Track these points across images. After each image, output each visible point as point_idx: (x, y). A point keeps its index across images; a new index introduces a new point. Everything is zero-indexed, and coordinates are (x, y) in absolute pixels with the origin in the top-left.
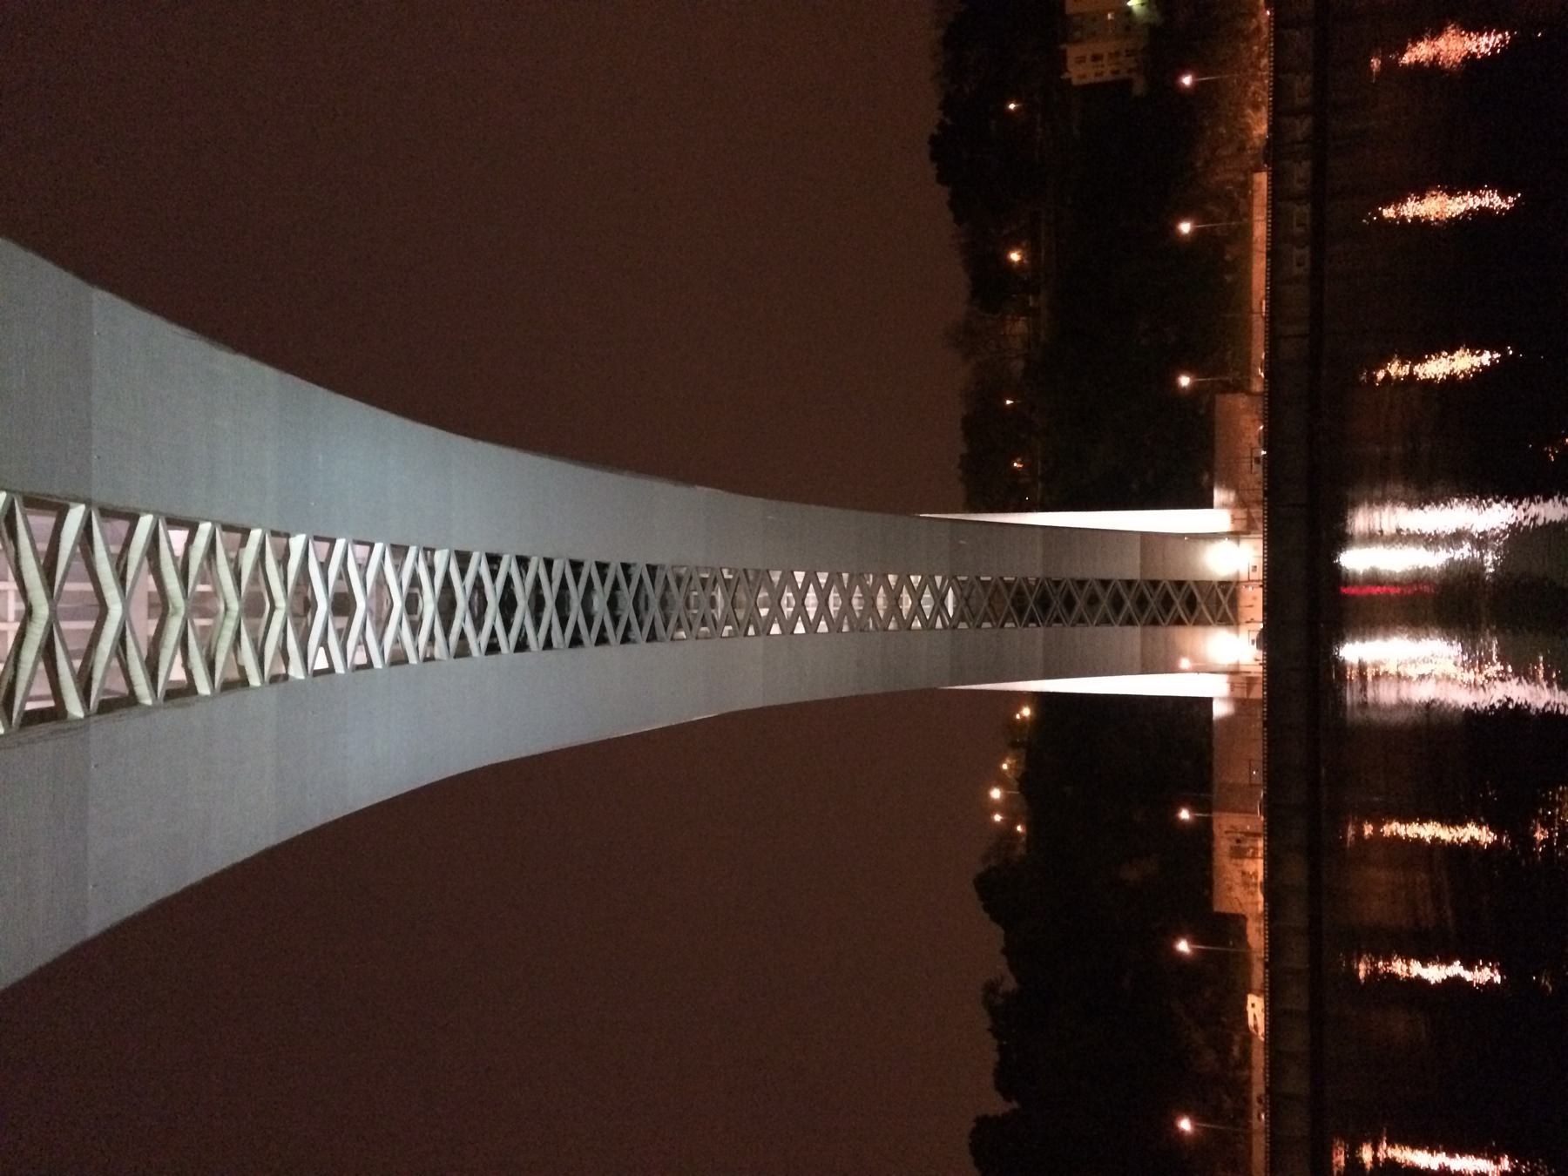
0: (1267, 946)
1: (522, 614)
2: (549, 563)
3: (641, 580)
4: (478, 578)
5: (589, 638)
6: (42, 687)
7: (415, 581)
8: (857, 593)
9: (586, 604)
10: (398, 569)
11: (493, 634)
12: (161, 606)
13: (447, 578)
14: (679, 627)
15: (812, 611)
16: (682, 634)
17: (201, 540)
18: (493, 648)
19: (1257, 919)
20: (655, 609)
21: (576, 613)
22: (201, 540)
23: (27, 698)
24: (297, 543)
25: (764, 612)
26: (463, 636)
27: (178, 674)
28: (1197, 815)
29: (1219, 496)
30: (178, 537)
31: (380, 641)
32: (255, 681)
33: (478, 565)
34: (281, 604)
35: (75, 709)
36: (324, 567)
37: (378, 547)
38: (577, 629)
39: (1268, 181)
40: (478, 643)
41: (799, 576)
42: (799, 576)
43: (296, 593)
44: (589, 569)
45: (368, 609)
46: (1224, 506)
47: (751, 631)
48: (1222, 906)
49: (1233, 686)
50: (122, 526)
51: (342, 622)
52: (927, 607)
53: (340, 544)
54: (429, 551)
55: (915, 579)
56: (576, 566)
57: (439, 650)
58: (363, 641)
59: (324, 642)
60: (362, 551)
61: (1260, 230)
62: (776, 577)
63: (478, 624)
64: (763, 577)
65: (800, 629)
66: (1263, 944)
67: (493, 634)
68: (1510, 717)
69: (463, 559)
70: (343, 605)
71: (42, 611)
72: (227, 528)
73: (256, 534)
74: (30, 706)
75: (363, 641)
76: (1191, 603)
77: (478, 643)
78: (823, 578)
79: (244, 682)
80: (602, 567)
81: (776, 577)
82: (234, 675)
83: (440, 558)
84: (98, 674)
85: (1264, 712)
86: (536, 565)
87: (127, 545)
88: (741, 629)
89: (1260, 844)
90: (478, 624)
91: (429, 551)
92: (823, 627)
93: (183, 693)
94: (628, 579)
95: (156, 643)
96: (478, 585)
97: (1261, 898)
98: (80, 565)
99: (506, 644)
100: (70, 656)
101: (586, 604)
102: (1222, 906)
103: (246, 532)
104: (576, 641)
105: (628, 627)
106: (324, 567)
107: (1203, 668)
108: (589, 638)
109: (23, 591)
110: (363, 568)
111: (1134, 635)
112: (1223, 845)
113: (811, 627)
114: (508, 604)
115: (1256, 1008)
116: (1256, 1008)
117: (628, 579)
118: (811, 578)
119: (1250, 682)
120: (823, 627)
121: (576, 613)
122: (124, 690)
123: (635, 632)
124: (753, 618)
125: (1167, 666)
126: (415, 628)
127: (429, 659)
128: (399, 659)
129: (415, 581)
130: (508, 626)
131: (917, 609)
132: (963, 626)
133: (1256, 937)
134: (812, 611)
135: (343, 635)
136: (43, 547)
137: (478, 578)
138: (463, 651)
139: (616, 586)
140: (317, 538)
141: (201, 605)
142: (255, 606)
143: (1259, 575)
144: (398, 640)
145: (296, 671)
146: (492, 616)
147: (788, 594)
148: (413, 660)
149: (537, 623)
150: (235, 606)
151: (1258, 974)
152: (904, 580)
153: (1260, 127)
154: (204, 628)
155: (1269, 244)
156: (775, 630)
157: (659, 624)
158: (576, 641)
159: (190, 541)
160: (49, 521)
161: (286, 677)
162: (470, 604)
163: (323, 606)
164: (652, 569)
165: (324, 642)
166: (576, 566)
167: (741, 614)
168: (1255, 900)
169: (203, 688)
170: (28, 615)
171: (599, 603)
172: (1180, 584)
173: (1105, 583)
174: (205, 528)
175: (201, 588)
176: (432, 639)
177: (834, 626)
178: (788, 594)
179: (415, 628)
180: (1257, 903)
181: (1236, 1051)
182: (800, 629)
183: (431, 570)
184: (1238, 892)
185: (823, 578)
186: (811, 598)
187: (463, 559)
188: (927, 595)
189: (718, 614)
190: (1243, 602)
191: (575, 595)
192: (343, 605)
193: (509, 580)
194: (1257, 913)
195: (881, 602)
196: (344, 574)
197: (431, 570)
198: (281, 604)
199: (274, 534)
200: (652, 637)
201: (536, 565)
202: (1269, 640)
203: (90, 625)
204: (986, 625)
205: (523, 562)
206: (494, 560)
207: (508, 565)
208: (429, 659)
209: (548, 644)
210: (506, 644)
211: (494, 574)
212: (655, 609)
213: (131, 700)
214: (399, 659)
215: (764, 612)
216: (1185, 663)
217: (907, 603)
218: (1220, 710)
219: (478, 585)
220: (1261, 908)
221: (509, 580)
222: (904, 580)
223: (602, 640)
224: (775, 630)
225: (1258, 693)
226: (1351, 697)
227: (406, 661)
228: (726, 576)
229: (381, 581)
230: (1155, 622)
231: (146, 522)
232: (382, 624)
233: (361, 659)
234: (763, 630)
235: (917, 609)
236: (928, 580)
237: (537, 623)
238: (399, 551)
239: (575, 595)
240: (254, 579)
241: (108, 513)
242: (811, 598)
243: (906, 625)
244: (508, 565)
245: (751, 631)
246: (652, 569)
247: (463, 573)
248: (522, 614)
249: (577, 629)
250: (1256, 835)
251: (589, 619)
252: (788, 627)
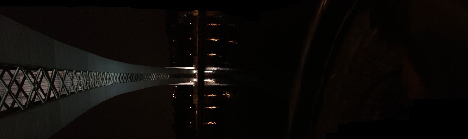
1: (126, 79)
2: (129, 74)
3: (138, 75)
4: (122, 76)
5: (133, 81)
6: (86, 87)
7: (116, 76)
8: (159, 75)
9: (132, 77)
10: (115, 75)
11: (124, 81)
12: (95, 79)
13: (119, 76)
14: (142, 79)
15: (155, 77)
16: (142, 80)
17: (98, 73)
18: (124, 82)
20: (139, 78)
21: (131, 79)
22: (98, 73)
23: (85, 88)
24: (105, 73)
25: (150, 78)
26: (121, 81)
27: (96, 85)
29: (194, 66)
30: (96, 73)
31: (113, 81)
32: (103, 86)
33: (122, 74)
34: (104, 79)
35: (89, 89)
36: (108, 75)
37: (113, 73)
38: (132, 80)
40: (122, 82)
41: (153, 74)
42: (153, 74)
43: (106, 78)
44: (133, 74)
45: (112, 79)
46: (194, 67)
47: (149, 80)
49: (195, 83)
50: (91, 73)
51: (110, 80)
52: (166, 77)
53: (109, 73)
54: (117, 73)
55: (165, 74)
56: (131, 74)
57: (119, 83)
58: (112, 82)
59: (108, 82)
60: (111, 73)
61: (197, 40)
62: (151, 74)
63: (122, 80)
64: (150, 74)
65: (154, 79)
67: (124, 81)
68: (219, 86)
69: (121, 74)
70: (110, 79)
71: (86, 81)
72: (100, 72)
73: (102, 72)
74: (85, 88)
75: (112, 82)
76: (191, 76)
77: (122, 82)
78: (156, 74)
79: (102, 86)
80: (134, 74)
81: (151, 74)
82: (101, 85)
83: (118, 74)
84: (90, 86)
86: (127, 74)
87: (92, 74)
88: (148, 79)
89: (197, 98)
90: (122, 80)
91: (117, 73)
92: (156, 79)
93: (97, 87)
94: (136, 75)
95: (95, 83)
96: (122, 76)
97: (197, 102)
98: (88, 77)
99: (125, 82)
100: (88, 84)
101: (132, 77)
103: (101, 72)
104: (132, 81)
105: (137, 80)
106: (108, 75)
107: (192, 82)
108: (133, 81)
109: (84, 79)
110: (111, 75)
111: (186, 79)
112: (194, 98)
113: (155, 79)
114: (125, 78)
115: (197, 112)
116: (197, 112)
117: (136, 75)
118: (155, 74)
119: (197, 83)
120: (156, 79)
121: (131, 79)
122: (92, 87)
123: (137, 80)
124: (149, 78)
125: (190, 82)
126: (116, 80)
127: (118, 83)
128: (115, 83)
129: (116, 76)
130: (125, 80)
131: (165, 77)
132: (170, 78)
133: (197, 106)
134: (155, 77)
135: (110, 81)
136: (85, 75)
137: (122, 76)
138: (121, 82)
139: (135, 76)
140: (107, 73)
141: (98, 79)
142: (102, 79)
143: (197, 73)
144: (115, 82)
145: (106, 85)
146: (124, 79)
147: (152, 76)
148: (116, 83)
149: (128, 80)
150: (101, 79)
151: (197, 109)
152: (164, 74)
153: (198, 30)
154: (98, 81)
156: (151, 79)
157: (140, 79)
158: (132, 81)
159: (97, 74)
160: (86, 73)
161: (105, 85)
162: (122, 78)
163: (108, 79)
164: (139, 74)
165: (108, 82)
166: (131, 74)
167: (148, 78)
169: (99, 87)
170: (85, 81)
171: (134, 77)
172: (190, 74)
173: (183, 74)
174: (98, 72)
175: (98, 78)
176: (118, 82)
177: (157, 79)
178: (152, 76)
179: (116, 80)
182: (154, 79)
183: (118, 75)
185: (156, 74)
186: (155, 76)
187: (121, 74)
188: (166, 75)
189: (146, 78)
190: (196, 76)
191: (131, 77)
192: (110, 79)
193: (125, 76)
195: (161, 76)
196: (110, 76)
197: (118, 75)
198: (104, 79)
199: (104, 72)
200: (139, 81)
201: (127, 74)
202: (199, 80)
203: (89, 81)
204: (172, 78)
205: (126, 74)
206: (124, 74)
207: (125, 74)
208: (118, 83)
209: (129, 82)
210: (125, 82)
211: (124, 75)
212: (139, 78)
213: (93, 88)
214: (115, 83)
215: (150, 78)
216: (191, 81)
217: (164, 76)
218: (194, 86)
219: (122, 76)
221: (125, 76)
222: (164, 74)
223: (134, 81)
224: (151, 79)
225: (197, 84)
226: (205, 84)
227: (116, 84)
228: (146, 74)
229: (113, 76)
230: (188, 78)
231: (93, 72)
232: (113, 80)
233: (112, 84)
234: (150, 79)
235: (165, 77)
236: (166, 74)
237: (128, 80)
238: (115, 73)
239: (131, 77)
240: (102, 77)
241: (90, 72)
242: (155, 76)
243: (164, 78)
244: (125, 74)
245: (149, 80)
246: (139, 74)
247: (121, 75)
248: (126, 79)
249: (132, 80)
250: (196, 97)
251: (133, 79)
252: (152, 79)
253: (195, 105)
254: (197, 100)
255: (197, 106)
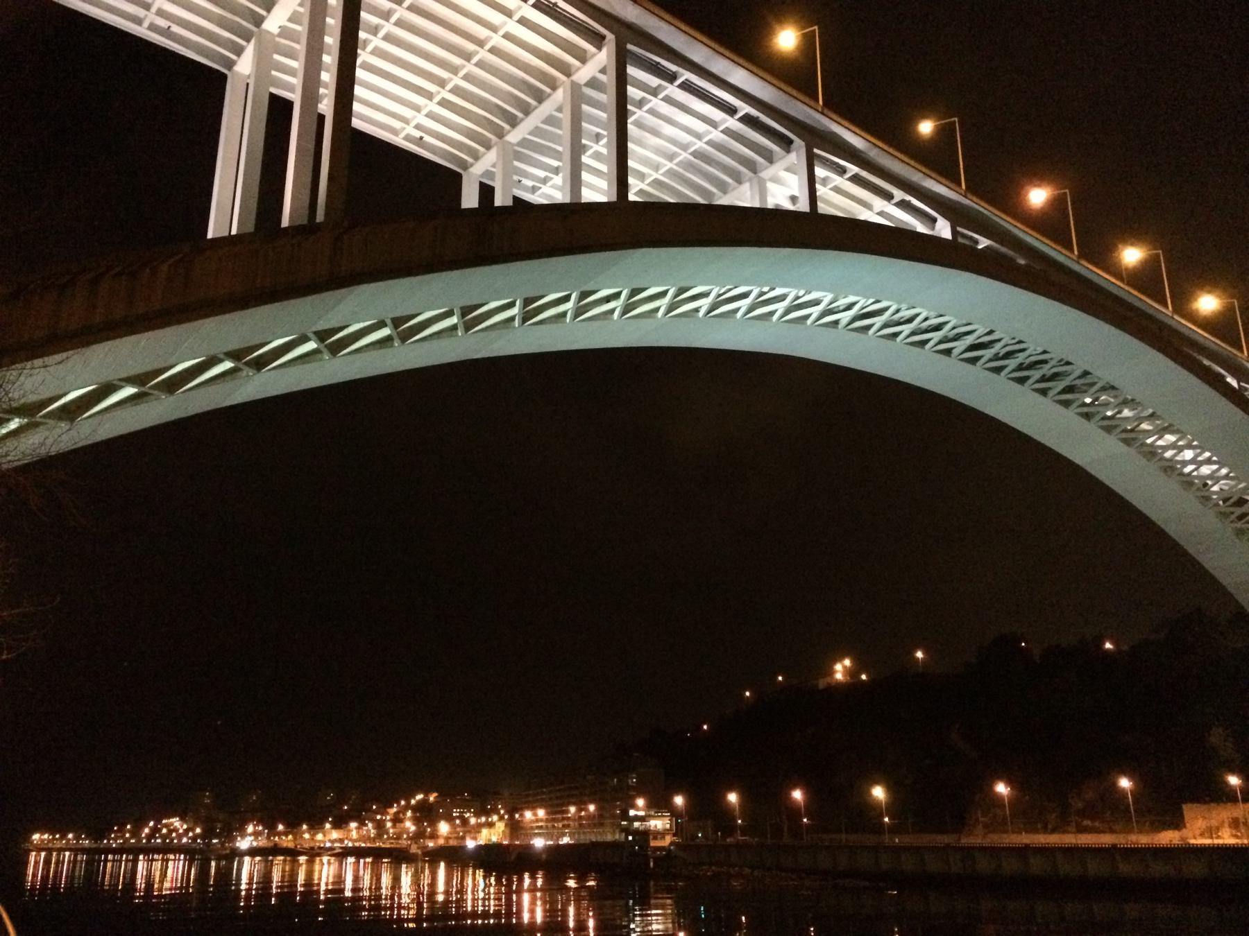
0: (1154, 846)
19: (1182, 839)
28: (1006, 798)
39: (1205, 844)
48: (1189, 810)
66: (1164, 843)
85: (1102, 844)
102: (1189, 810)
133: (1168, 838)
155: (1176, 846)
168: (1197, 837)
180: (1195, 838)
181: (1087, 823)
184: (1200, 824)
194: (1187, 838)
220: (1193, 841)
253: (1177, 823)
254: (1227, 838)
255: (1168, 838)
